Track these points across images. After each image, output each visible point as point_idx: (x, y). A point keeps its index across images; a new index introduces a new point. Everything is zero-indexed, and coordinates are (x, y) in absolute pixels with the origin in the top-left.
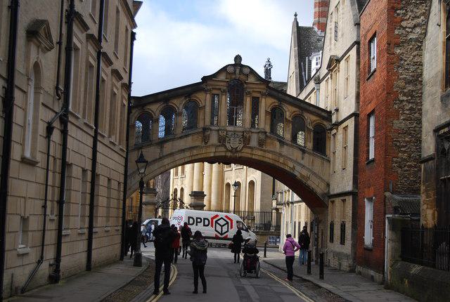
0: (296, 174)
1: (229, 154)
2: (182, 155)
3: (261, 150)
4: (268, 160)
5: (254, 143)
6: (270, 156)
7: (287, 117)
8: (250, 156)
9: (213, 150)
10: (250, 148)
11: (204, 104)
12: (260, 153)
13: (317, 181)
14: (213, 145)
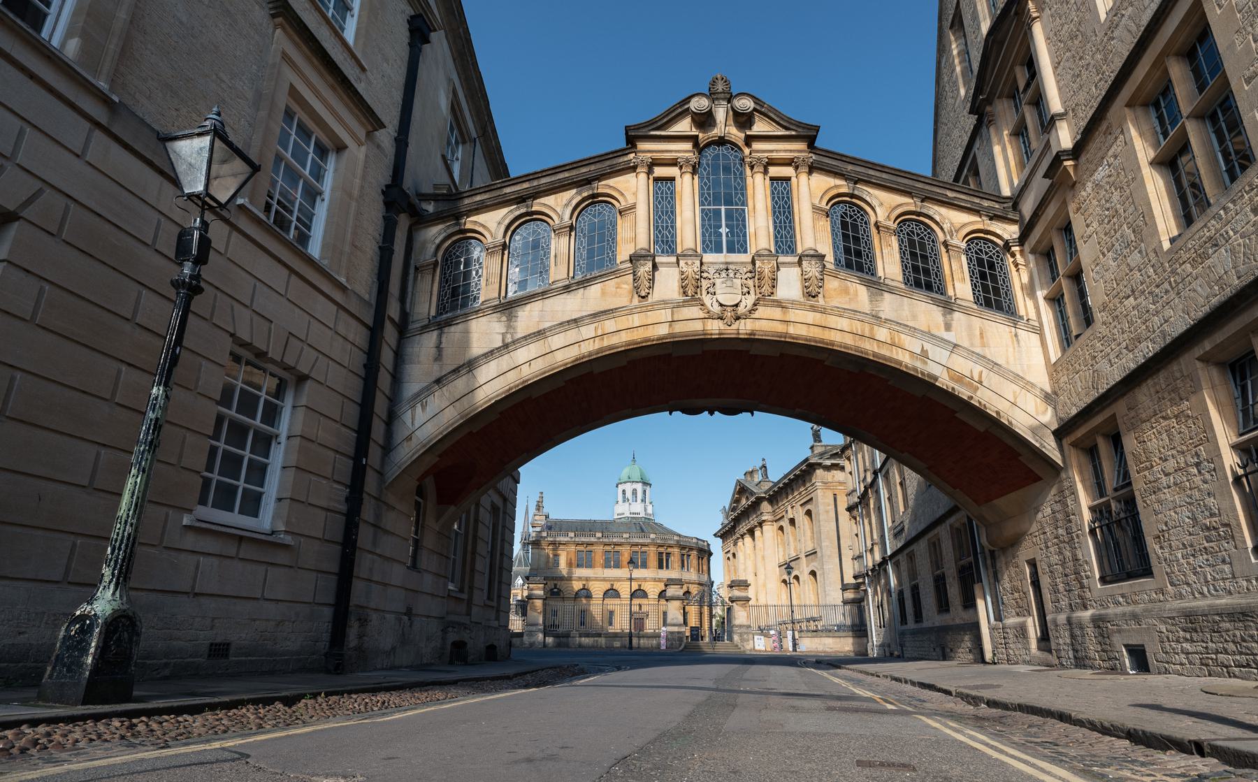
0: (933, 369)
1: (715, 327)
2: (571, 335)
3: (813, 309)
4: (836, 337)
5: (789, 284)
6: (844, 323)
7: (880, 219)
8: (780, 328)
9: (665, 315)
10: (779, 304)
11: (631, 201)
12: (811, 317)
13: (1009, 390)
14: (665, 302)
